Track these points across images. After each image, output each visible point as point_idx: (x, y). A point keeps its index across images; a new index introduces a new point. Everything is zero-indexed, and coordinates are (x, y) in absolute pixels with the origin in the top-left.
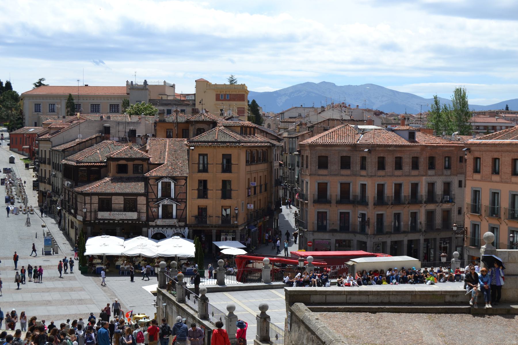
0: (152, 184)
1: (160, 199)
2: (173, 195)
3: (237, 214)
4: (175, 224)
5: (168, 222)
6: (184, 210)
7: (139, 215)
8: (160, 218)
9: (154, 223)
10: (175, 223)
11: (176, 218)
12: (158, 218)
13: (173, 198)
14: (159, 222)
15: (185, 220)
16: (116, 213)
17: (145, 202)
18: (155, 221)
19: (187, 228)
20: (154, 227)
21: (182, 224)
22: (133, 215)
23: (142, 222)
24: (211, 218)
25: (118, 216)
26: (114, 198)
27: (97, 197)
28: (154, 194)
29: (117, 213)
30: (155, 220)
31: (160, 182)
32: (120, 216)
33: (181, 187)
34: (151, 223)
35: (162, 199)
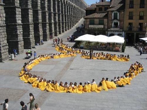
2: (118, 18)
12: (112, 27)
14: (112, 29)
15: (123, 29)
17: (107, 21)
19: (123, 32)
20: (110, 31)
21: (122, 30)
22: (102, 26)
26: (95, 19)
34: (109, 30)
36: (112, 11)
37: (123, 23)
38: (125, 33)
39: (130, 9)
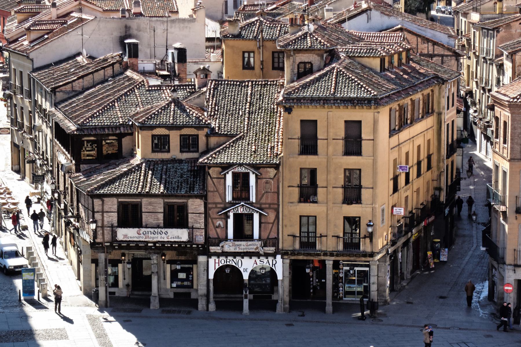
0: (215, 176)
1: (230, 203)
2: (253, 198)
3: (372, 233)
4: (257, 251)
5: (243, 246)
6: (273, 223)
7: (191, 235)
8: (230, 240)
9: (218, 248)
10: (257, 248)
11: (260, 239)
12: (226, 239)
13: (254, 201)
14: (229, 247)
15: (275, 242)
16: (149, 230)
17: (202, 209)
18: (220, 245)
19: (279, 257)
20: (218, 255)
21: (271, 250)
23: (198, 245)
24: (324, 239)
25: (152, 235)
27: (115, 200)
28: (219, 193)
29: (152, 230)
30: (221, 241)
31: (230, 173)
32: (156, 235)
33: (267, 183)
34: (213, 249)
35: (234, 204)
36: (226, 167)
37: (277, 217)
38: (288, 261)
39: (304, 158)
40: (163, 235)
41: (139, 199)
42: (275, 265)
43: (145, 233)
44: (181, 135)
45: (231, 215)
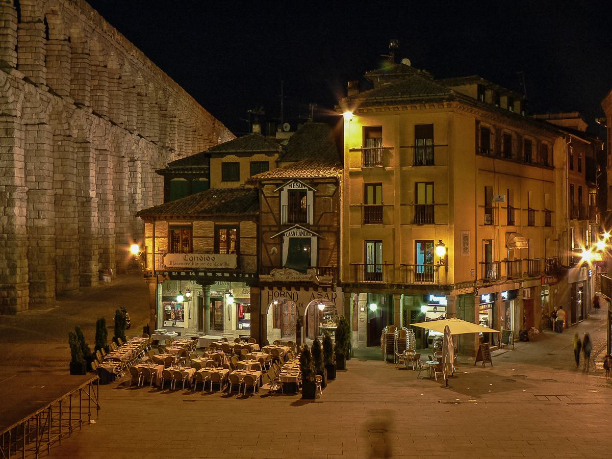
0: (269, 195)
2: (310, 220)
4: (312, 280)
9: (269, 276)
11: (317, 268)
17: (255, 234)
21: (328, 279)
25: (199, 262)
28: (273, 214)
30: (272, 268)
34: (263, 277)
40: (211, 261)
41: (189, 222)
42: (334, 299)
43: (191, 259)
44: (251, 163)
45: (286, 239)
